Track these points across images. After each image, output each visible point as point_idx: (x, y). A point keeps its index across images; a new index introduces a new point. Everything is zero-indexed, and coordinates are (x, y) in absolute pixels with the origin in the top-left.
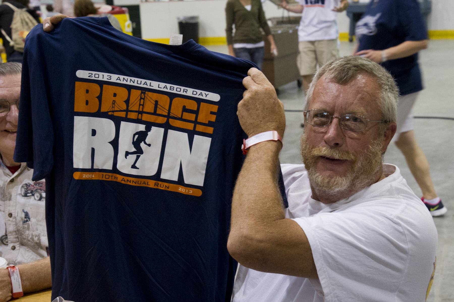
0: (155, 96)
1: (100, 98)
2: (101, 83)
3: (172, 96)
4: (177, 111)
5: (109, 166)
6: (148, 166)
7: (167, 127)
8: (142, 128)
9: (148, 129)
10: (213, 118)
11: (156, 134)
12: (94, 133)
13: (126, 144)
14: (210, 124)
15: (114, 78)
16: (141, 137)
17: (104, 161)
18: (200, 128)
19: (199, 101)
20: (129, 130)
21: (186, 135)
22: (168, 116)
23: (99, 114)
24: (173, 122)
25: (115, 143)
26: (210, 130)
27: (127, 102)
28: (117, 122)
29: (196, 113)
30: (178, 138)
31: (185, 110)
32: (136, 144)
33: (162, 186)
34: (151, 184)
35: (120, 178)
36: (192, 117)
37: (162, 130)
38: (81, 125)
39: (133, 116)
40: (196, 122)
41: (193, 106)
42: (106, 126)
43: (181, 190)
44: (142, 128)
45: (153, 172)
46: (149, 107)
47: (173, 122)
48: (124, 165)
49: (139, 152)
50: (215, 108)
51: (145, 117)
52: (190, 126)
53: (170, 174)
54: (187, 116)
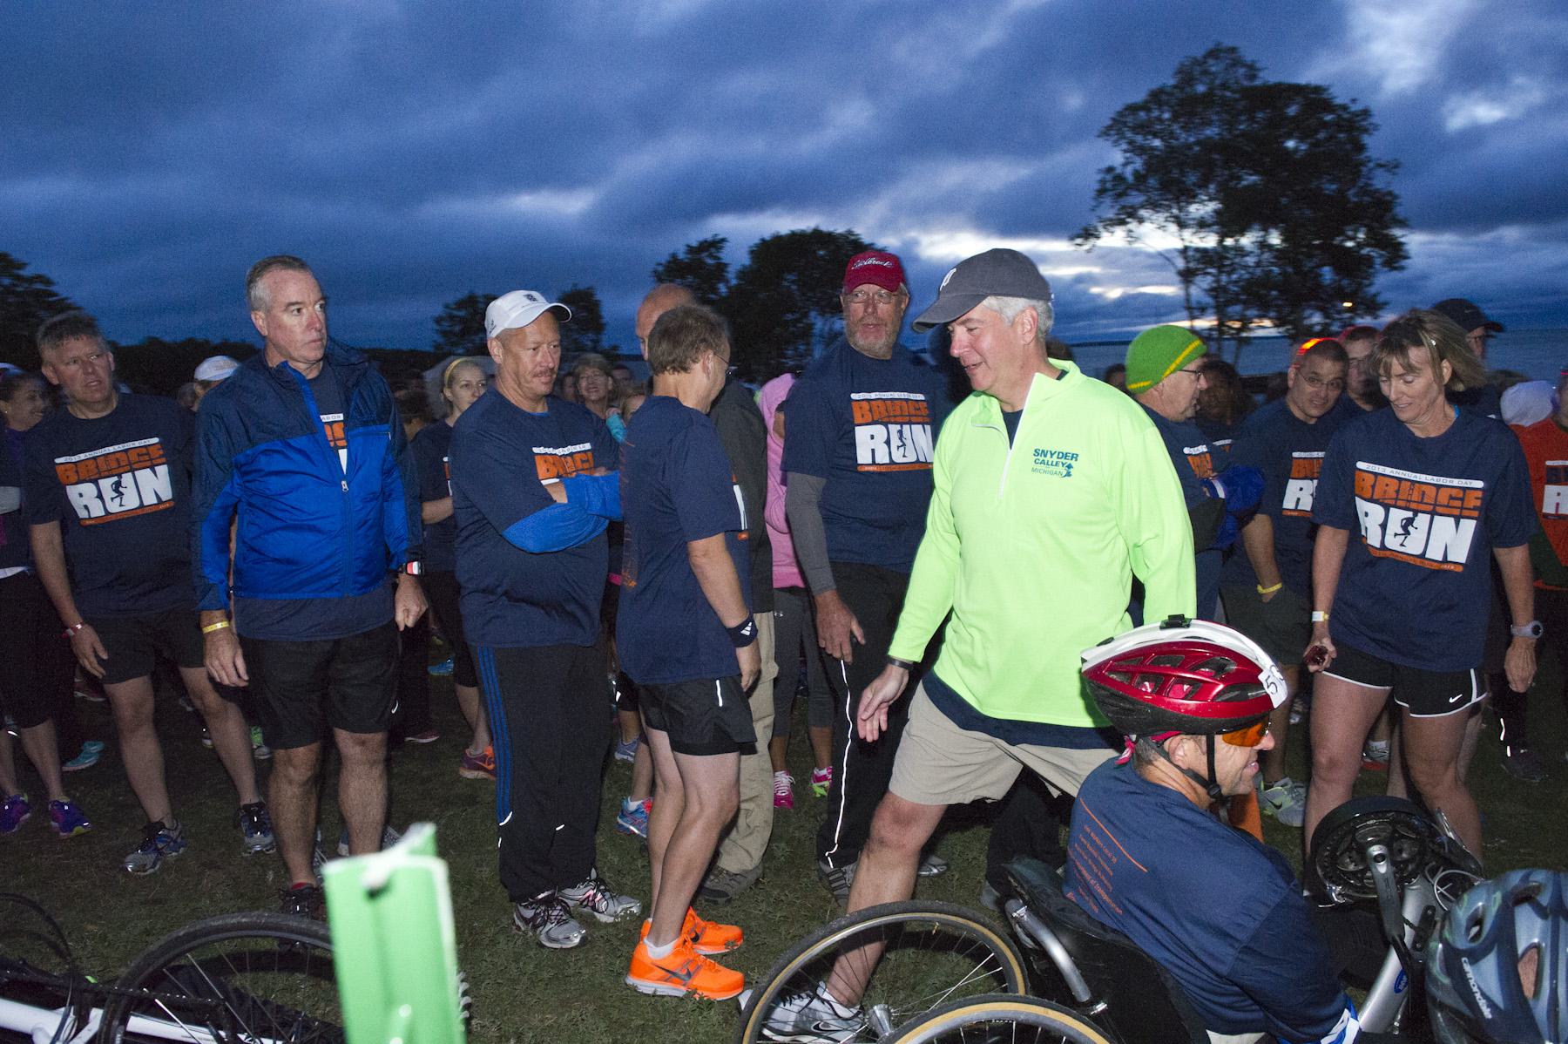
0: (1424, 488)
1: (1373, 487)
3: (1439, 487)
4: (1443, 499)
5: (1378, 545)
7: (1433, 513)
8: (1410, 514)
9: (1415, 515)
10: (1478, 503)
14: (1475, 508)
15: (1388, 471)
16: (1410, 521)
18: (1466, 513)
19: (1465, 489)
20: (1397, 515)
21: (1452, 520)
22: (1435, 505)
24: (1439, 509)
26: (1476, 514)
27: (1397, 492)
28: (1387, 508)
29: (1462, 500)
31: (1451, 498)
32: (1405, 528)
33: (1427, 565)
36: (1458, 503)
40: (1462, 508)
43: (1445, 567)
44: (1410, 514)
45: (1418, 551)
46: (1416, 496)
47: (1439, 509)
49: (1407, 533)
50: (1480, 494)
51: (1413, 506)
52: (1457, 512)
53: (1435, 553)
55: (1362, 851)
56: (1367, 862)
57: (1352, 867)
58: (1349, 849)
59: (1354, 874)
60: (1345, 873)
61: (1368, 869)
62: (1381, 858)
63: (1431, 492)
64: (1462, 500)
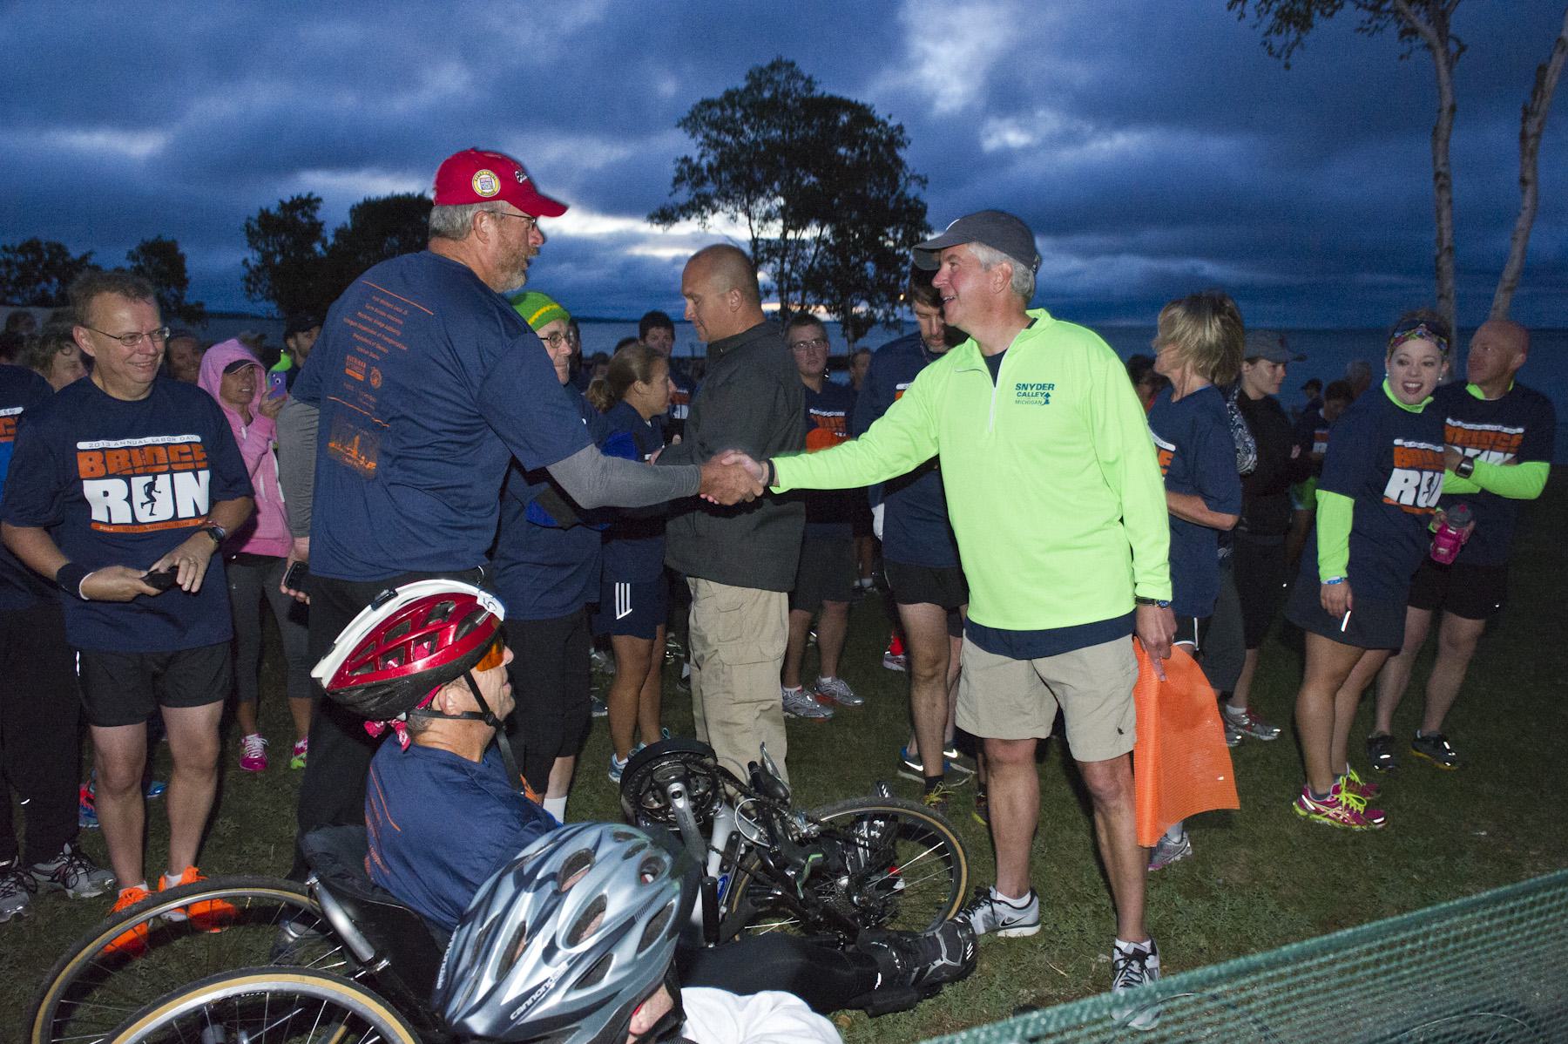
2: (102, 450)
5: (129, 520)
6: (163, 511)
7: (171, 472)
8: (150, 479)
11: (163, 481)
12: (106, 494)
13: (139, 496)
16: (151, 487)
17: (122, 515)
18: (199, 465)
20: (139, 483)
23: (108, 476)
24: (175, 467)
25: (129, 499)
30: (184, 480)
31: (181, 454)
32: (149, 494)
34: (173, 525)
35: (138, 530)
36: (190, 458)
37: (168, 476)
38: (92, 489)
39: (142, 470)
40: (194, 461)
41: (186, 449)
42: (117, 487)
44: (150, 479)
45: (170, 515)
47: (175, 467)
48: (143, 516)
49: (153, 500)
52: (191, 466)
54: (185, 458)
55: (663, 788)
56: (667, 799)
57: (656, 805)
58: (650, 789)
59: (659, 810)
60: (651, 811)
61: (669, 805)
62: (679, 794)
63: (163, 451)
64: (191, 453)
